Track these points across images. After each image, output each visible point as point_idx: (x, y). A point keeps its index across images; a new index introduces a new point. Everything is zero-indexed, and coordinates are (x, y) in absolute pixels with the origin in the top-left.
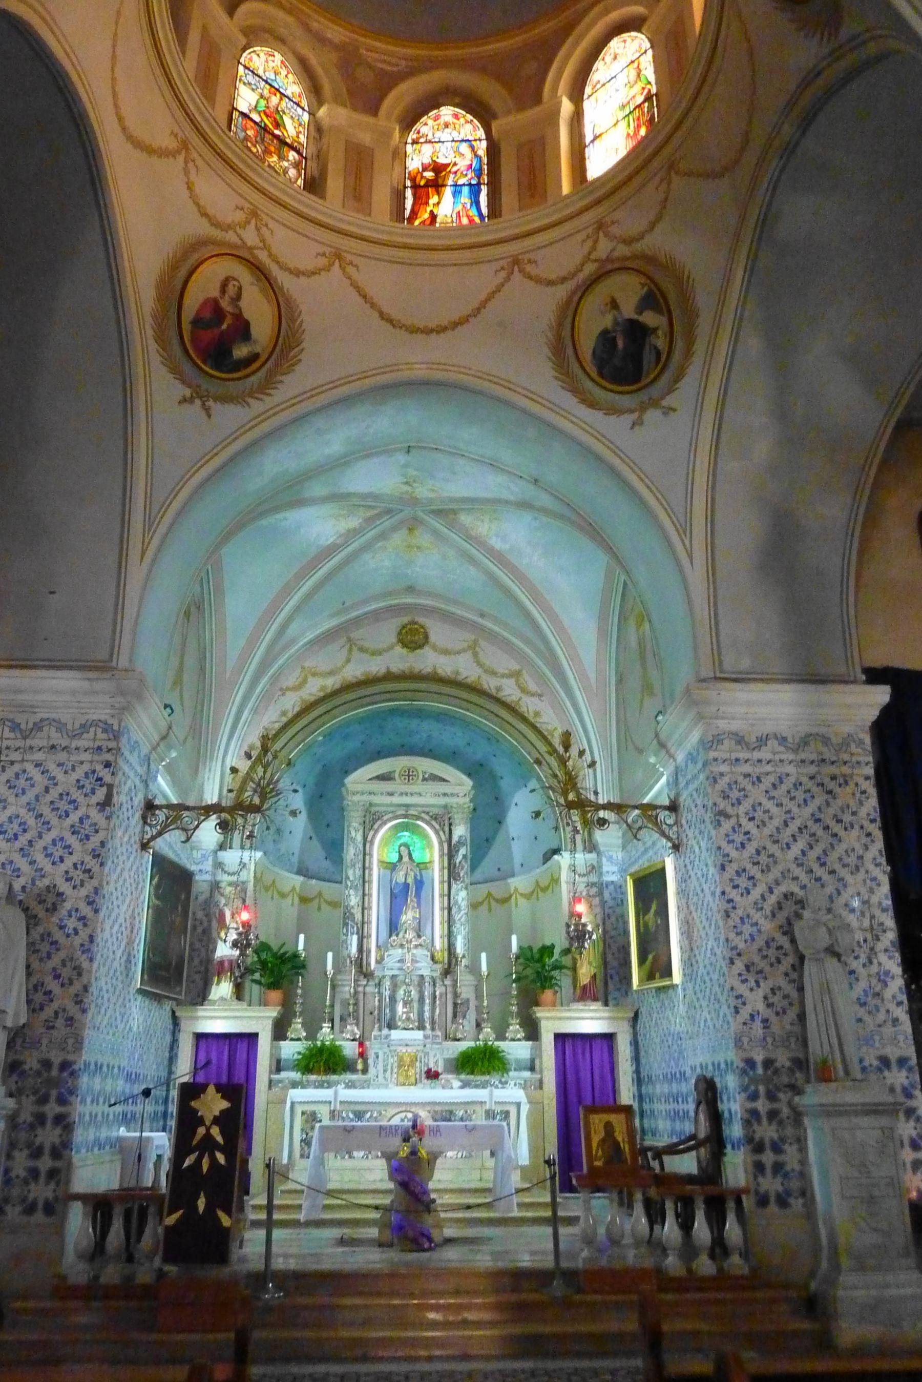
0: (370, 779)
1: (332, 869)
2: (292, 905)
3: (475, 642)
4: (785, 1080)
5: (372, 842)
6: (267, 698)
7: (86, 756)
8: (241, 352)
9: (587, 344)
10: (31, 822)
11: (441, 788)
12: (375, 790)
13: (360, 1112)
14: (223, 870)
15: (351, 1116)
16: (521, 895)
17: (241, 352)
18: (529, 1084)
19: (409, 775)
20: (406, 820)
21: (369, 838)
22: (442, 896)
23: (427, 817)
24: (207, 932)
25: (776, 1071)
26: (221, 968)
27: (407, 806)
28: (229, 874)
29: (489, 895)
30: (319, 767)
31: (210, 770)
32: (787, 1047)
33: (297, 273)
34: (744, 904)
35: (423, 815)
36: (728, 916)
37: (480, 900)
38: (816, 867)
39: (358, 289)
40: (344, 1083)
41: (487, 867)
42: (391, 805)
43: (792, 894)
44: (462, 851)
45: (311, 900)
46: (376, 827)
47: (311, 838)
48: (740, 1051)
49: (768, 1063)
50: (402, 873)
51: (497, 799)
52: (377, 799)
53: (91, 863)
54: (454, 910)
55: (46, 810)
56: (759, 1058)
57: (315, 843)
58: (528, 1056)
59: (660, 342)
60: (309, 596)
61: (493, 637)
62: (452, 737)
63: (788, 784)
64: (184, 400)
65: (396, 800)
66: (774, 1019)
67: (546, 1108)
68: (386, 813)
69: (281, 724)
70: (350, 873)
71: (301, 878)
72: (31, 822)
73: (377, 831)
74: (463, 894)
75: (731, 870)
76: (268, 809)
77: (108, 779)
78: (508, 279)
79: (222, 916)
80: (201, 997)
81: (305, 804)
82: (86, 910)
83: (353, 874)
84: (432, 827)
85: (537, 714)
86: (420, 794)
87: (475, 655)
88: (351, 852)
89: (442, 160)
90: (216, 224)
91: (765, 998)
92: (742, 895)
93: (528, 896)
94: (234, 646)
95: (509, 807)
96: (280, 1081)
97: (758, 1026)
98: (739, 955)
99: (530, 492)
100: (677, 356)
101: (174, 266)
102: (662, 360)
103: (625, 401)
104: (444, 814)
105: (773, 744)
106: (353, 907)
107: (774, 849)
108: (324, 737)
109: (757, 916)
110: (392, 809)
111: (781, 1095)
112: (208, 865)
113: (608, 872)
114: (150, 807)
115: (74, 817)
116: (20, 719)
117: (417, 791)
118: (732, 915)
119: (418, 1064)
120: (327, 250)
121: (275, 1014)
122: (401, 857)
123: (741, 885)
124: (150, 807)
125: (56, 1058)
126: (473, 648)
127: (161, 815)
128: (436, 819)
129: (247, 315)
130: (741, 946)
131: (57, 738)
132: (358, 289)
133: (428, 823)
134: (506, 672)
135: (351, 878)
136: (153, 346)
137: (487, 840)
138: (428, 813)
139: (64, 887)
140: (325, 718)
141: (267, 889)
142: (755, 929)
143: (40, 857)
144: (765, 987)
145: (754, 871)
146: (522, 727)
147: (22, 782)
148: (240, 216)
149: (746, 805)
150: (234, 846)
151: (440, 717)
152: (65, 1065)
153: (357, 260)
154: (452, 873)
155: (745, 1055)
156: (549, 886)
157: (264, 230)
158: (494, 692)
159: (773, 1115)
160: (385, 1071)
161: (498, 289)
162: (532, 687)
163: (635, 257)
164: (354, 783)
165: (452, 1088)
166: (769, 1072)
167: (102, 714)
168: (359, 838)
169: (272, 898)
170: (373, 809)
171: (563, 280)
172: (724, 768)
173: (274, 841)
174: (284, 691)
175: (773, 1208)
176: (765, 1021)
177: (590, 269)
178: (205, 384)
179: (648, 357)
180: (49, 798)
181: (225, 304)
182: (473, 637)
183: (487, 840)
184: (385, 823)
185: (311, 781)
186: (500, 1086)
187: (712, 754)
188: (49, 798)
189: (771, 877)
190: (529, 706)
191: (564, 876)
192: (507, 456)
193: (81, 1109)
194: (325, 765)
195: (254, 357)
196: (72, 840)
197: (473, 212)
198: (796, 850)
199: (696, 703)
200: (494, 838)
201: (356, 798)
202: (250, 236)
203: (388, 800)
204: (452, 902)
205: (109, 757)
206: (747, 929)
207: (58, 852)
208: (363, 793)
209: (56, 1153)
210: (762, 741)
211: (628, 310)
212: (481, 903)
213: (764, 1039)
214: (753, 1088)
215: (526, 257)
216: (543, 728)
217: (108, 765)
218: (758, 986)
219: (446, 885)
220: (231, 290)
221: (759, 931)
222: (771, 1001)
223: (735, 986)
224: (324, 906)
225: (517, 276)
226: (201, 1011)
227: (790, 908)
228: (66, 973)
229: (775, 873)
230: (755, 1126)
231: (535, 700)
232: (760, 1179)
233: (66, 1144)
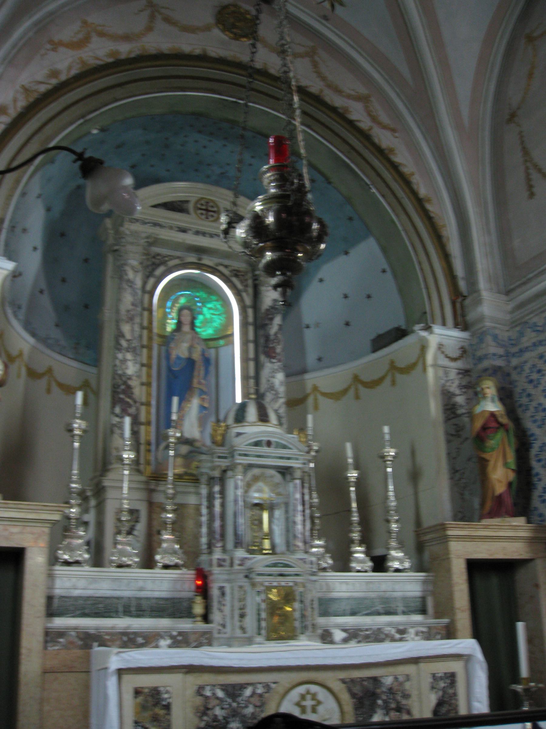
13: (234, 686)
15: (220, 694)
16: (324, 395)
21: (149, 287)
22: (245, 377)
27: (200, 250)
35: (221, 268)
40: (172, 637)
44: (278, 320)
50: (185, 346)
52: (165, 234)
54: (269, 397)
58: (418, 594)
65: (190, 239)
69: (49, 87)
70: (126, 329)
71: (32, 340)
74: (280, 377)
84: (232, 286)
85: (392, 150)
93: (336, 396)
96: (61, 633)
104: (246, 273)
106: (130, 378)
108: (102, 130)
113: (494, 355)
119: (297, 605)
122: (179, 324)
128: (236, 276)
133: (227, 280)
134: (353, 93)
135: (128, 336)
138: (226, 267)
140: (118, 92)
146: (376, 163)
156: (381, 380)
160: (242, 616)
162: (384, 118)
165: (332, 642)
168: (139, 282)
170: (155, 250)
174: (56, 46)
186: (398, 636)
208: (144, 223)
219: (252, 364)
224: (55, 389)
231: (388, 134)
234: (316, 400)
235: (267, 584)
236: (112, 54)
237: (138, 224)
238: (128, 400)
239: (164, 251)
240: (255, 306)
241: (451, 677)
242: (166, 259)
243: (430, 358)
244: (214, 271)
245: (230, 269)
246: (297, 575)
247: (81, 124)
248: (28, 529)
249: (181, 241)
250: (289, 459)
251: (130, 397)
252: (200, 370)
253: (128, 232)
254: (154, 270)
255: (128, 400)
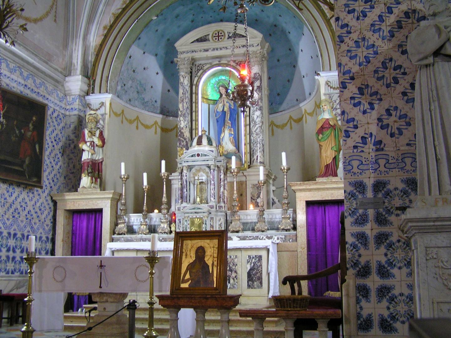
0: (192, 42)
2: (156, 133)
4: (398, 202)
5: (197, 86)
12: (196, 49)
14: (90, 108)
16: (308, 114)
18: (288, 238)
19: (218, 36)
20: (220, 68)
21: (195, 83)
23: (234, 64)
25: (388, 194)
27: (220, 57)
28: (94, 110)
29: (291, 117)
31: (76, 44)
32: (402, 168)
36: (342, 41)
37: (285, 122)
42: (207, 58)
43: (414, 11)
45: (172, 130)
46: (199, 74)
47: (169, 91)
48: (349, 175)
49: (378, 186)
51: (290, 50)
52: (197, 55)
65: (210, 54)
66: (387, 140)
67: (299, 255)
68: (206, 64)
71: (161, 116)
73: (200, 78)
76: (7, 27)
81: (160, 67)
86: (227, 48)
91: (380, 120)
92: (358, 19)
95: (298, 53)
97: (370, 148)
98: (352, 78)
108: (157, 16)
109: (373, 38)
110: (210, 61)
111: (392, 218)
112: (77, 104)
117: (225, 46)
118: (346, 40)
121: (111, 196)
122: (221, 95)
123: (357, 9)
130: (355, 69)
137: (289, 81)
141: (131, 122)
142: (371, 51)
144: (379, 109)
150: (95, 91)
155: (354, 179)
159: (381, 239)
164: (181, 46)
166: (380, 195)
169: (137, 128)
170: (197, 63)
173: (138, 92)
175: (376, 330)
176: (378, 143)
183: (289, 81)
184: (205, 72)
194: (168, 40)
200: (292, 79)
201: (182, 56)
204: (251, 119)
206: (362, 53)
208: (188, 52)
212: (286, 124)
213: (376, 162)
214: (361, 211)
218: (372, 108)
221: (376, 53)
222: (385, 122)
223: (347, 110)
230: (362, 251)
232: (363, 303)
234: (306, 117)
235: (191, 217)
237: (185, 54)
238: (181, 139)
239: (202, 62)
241: (260, 257)
242: (204, 65)
243: (323, 90)
244: (227, 65)
245: (237, 62)
246: (204, 213)
247: (137, 21)
248: (103, 201)
249: (206, 56)
250: (208, 160)
251: (183, 138)
252: (228, 116)
253: (179, 60)
254: (198, 72)
255: (181, 139)
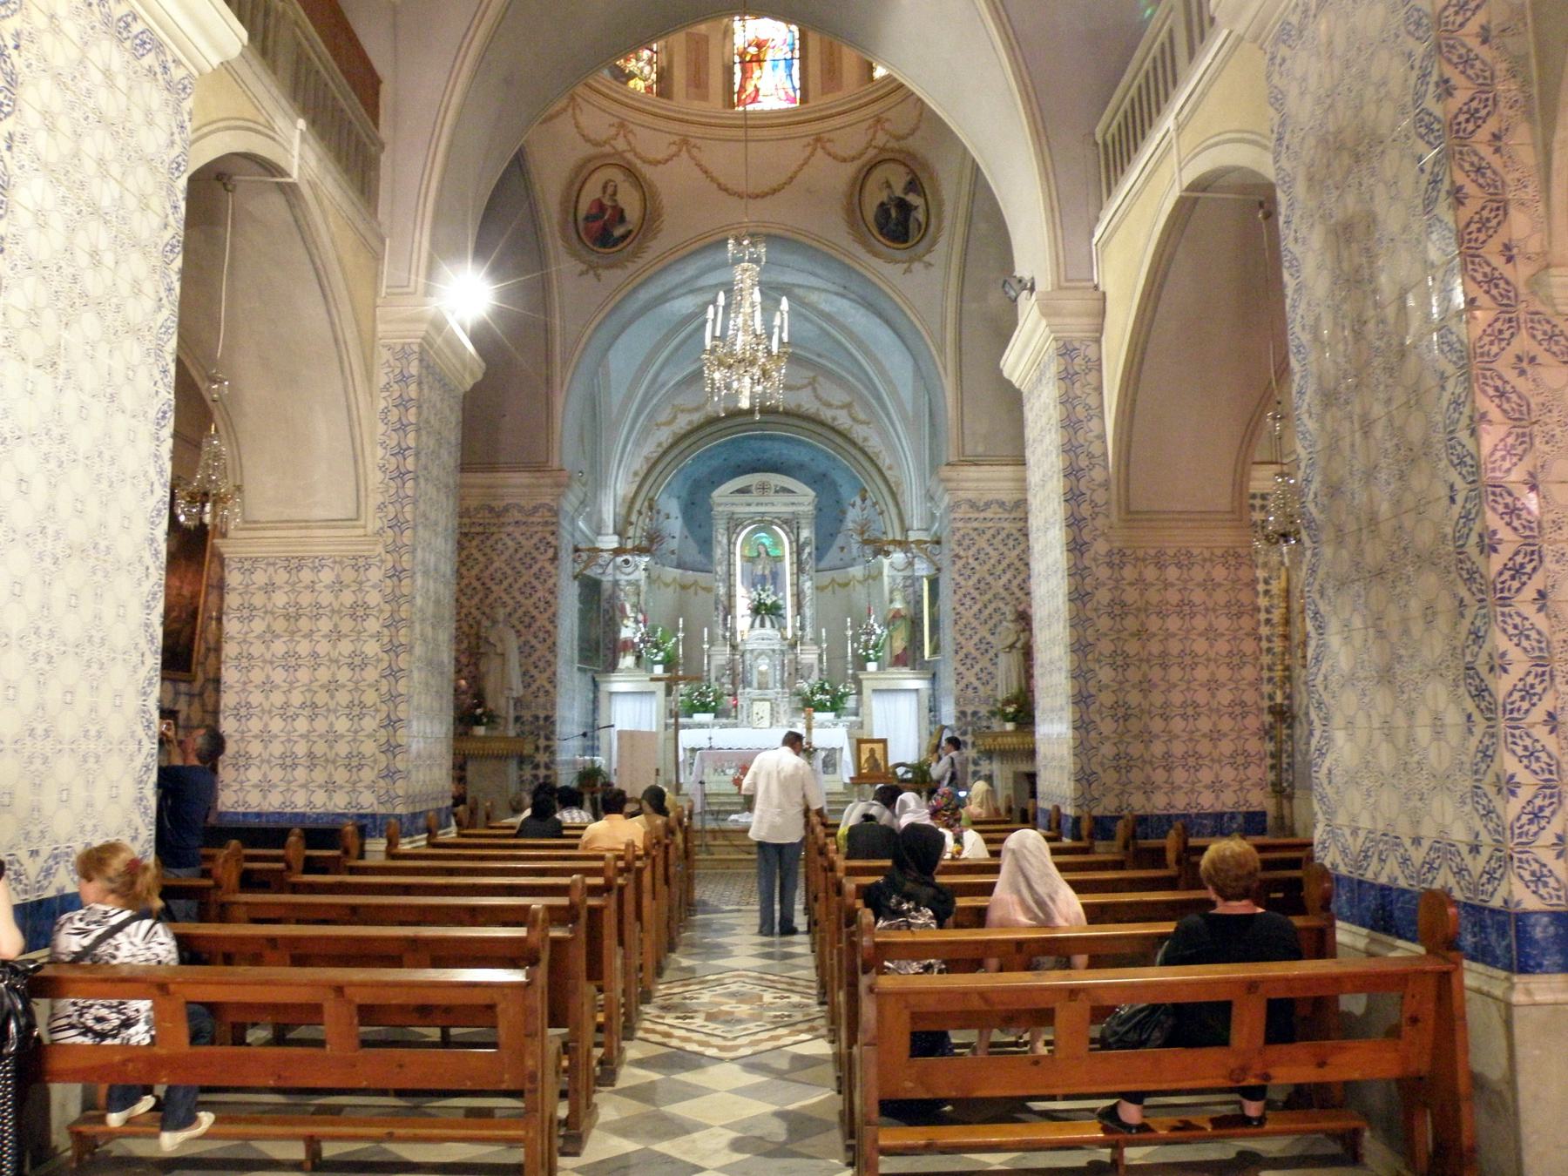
1: (705, 561)
3: (814, 379)
6: (646, 432)
7: (540, 528)
8: (619, 231)
9: (870, 210)
10: (509, 572)
11: (791, 499)
17: (619, 231)
19: (763, 488)
24: (612, 619)
26: (628, 646)
29: (833, 580)
30: (689, 482)
33: (656, 163)
34: (968, 615)
38: (1016, 590)
39: (699, 165)
41: (832, 556)
44: (807, 550)
49: (975, 714)
53: (550, 597)
55: (518, 565)
56: (969, 710)
57: (690, 541)
59: (920, 215)
60: (677, 349)
61: (829, 374)
62: (796, 455)
63: (1003, 534)
64: (582, 274)
65: (753, 509)
72: (509, 572)
75: (960, 593)
77: (554, 543)
78: (812, 154)
79: (623, 610)
80: (612, 667)
82: (550, 627)
83: (721, 569)
85: (865, 439)
87: (814, 389)
88: (718, 552)
89: (762, 37)
90: (596, 144)
94: (616, 399)
97: (970, 691)
99: (841, 290)
100: (932, 228)
101: (571, 183)
102: (924, 229)
103: (898, 254)
105: (995, 507)
107: (990, 579)
114: (577, 550)
115: (536, 568)
116: (494, 504)
120: (676, 138)
124: (577, 550)
125: (542, 715)
126: (812, 383)
127: (584, 556)
129: (622, 204)
131: (518, 516)
132: (699, 165)
136: (560, 243)
139: (535, 613)
143: (517, 594)
145: (975, 594)
146: (854, 452)
147: (499, 546)
148: (613, 131)
149: (974, 550)
151: (787, 440)
152: (547, 718)
153: (699, 142)
154: (800, 568)
157: (630, 136)
158: (829, 421)
161: (806, 162)
162: (862, 416)
163: (900, 151)
167: (547, 500)
168: (725, 541)
171: (853, 159)
172: (960, 524)
177: (872, 152)
178: (594, 258)
179: (912, 226)
180: (518, 556)
181: (607, 202)
182: (811, 374)
185: (684, 494)
187: (953, 516)
188: (518, 556)
189: (986, 597)
190: (859, 432)
191: (886, 571)
192: (820, 271)
193: (558, 744)
195: (630, 232)
196: (535, 583)
197: (788, 85)
198: (1004, 579)
199: (942, 480)
202: (621, 144)
203: (747, 509)
205: (552, 528)
207: (528, 591)
209: (547, 767)
210: (988, 505)
211: (899, 193)
215: (826, 136)
216: (870, 451)
217: (553, 533)
220: (610, 190)
225: (820, 152)
226: (614, 677)
227: (997, 617)
228: (541, 664)
229: (989, 596)
231: (864, 427)
233: (553, 762)
236: (690, 422)
240: (797, 540)
